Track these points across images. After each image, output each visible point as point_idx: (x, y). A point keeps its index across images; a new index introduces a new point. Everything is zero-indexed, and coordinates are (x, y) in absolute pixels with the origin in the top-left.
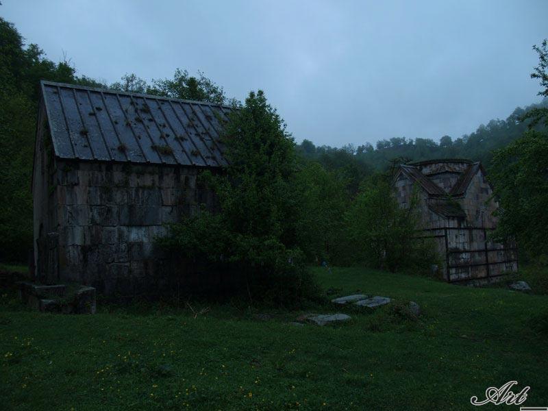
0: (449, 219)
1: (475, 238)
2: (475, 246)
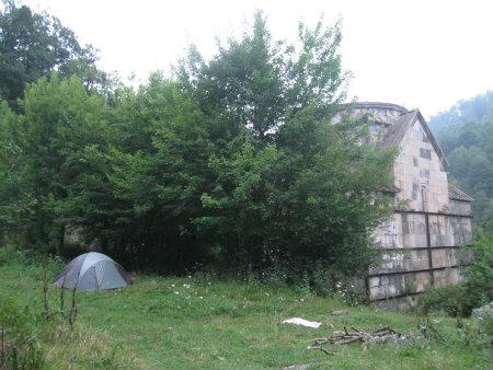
1: (411, 228)
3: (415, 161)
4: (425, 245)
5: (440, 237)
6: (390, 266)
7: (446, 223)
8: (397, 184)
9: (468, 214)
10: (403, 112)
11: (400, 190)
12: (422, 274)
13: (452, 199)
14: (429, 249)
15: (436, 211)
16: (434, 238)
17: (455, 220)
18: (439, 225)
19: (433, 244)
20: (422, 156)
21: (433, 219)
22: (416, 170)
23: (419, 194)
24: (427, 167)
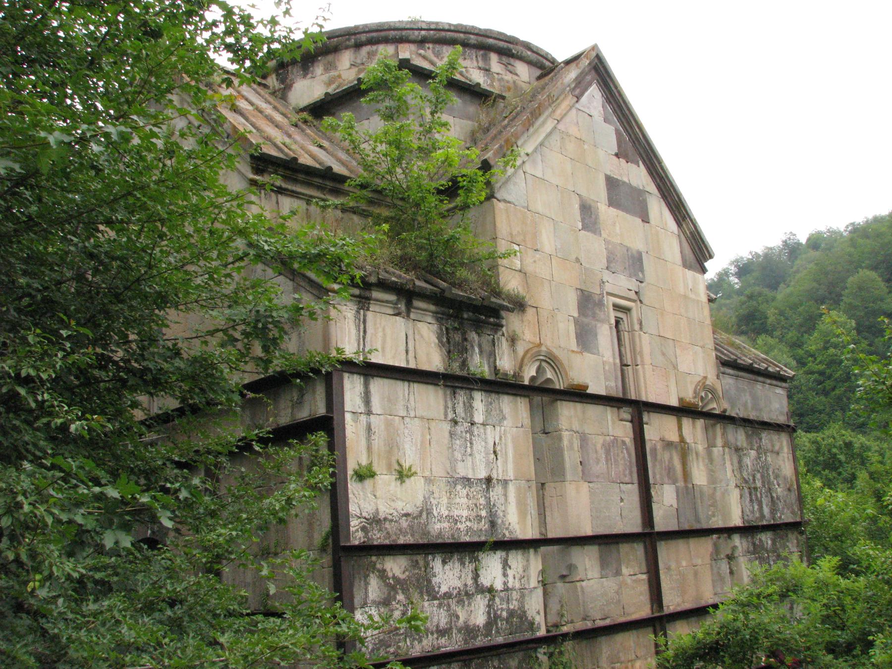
0: (363, 302)
1: (571, 458)
2: (584, 507)
3: (587, 209)
4: (632, 523)
5: (688, 492)
6: (477, 614)
7: (711, 445)
8: (511, 283)
9: (782, 419)
10: (545, 67)
11: (519, 305)
12: (628, 641)
13: (729, 364)
14: (650, 538)
15: (674, 402)
16: (666, 498)
17: (739, 436)
18: (683, 449)
19: (661, 523)
20: (613, 202)
21: (659, 429)
22: (594, 249)
23: (605, 336)
24: (637, 244)
